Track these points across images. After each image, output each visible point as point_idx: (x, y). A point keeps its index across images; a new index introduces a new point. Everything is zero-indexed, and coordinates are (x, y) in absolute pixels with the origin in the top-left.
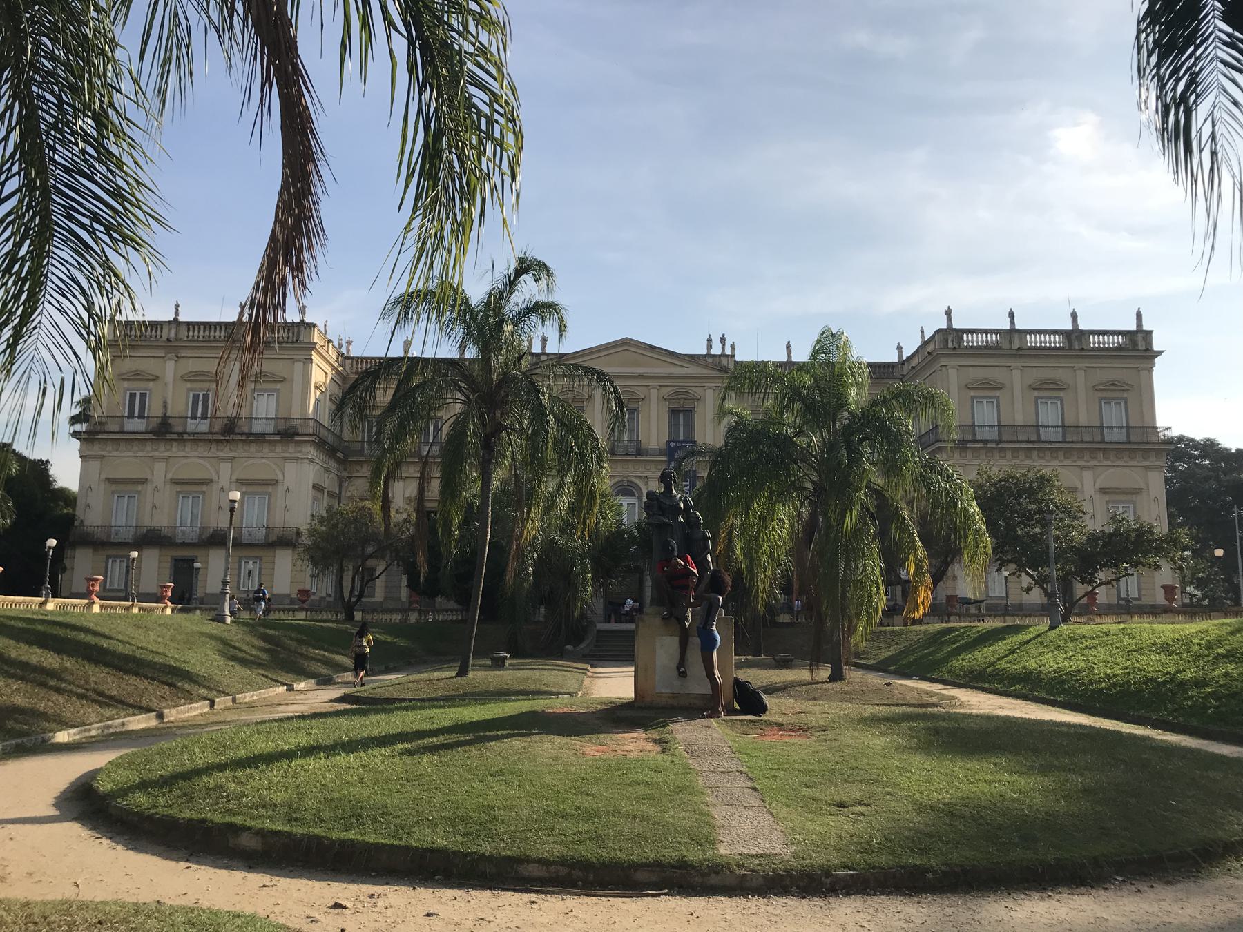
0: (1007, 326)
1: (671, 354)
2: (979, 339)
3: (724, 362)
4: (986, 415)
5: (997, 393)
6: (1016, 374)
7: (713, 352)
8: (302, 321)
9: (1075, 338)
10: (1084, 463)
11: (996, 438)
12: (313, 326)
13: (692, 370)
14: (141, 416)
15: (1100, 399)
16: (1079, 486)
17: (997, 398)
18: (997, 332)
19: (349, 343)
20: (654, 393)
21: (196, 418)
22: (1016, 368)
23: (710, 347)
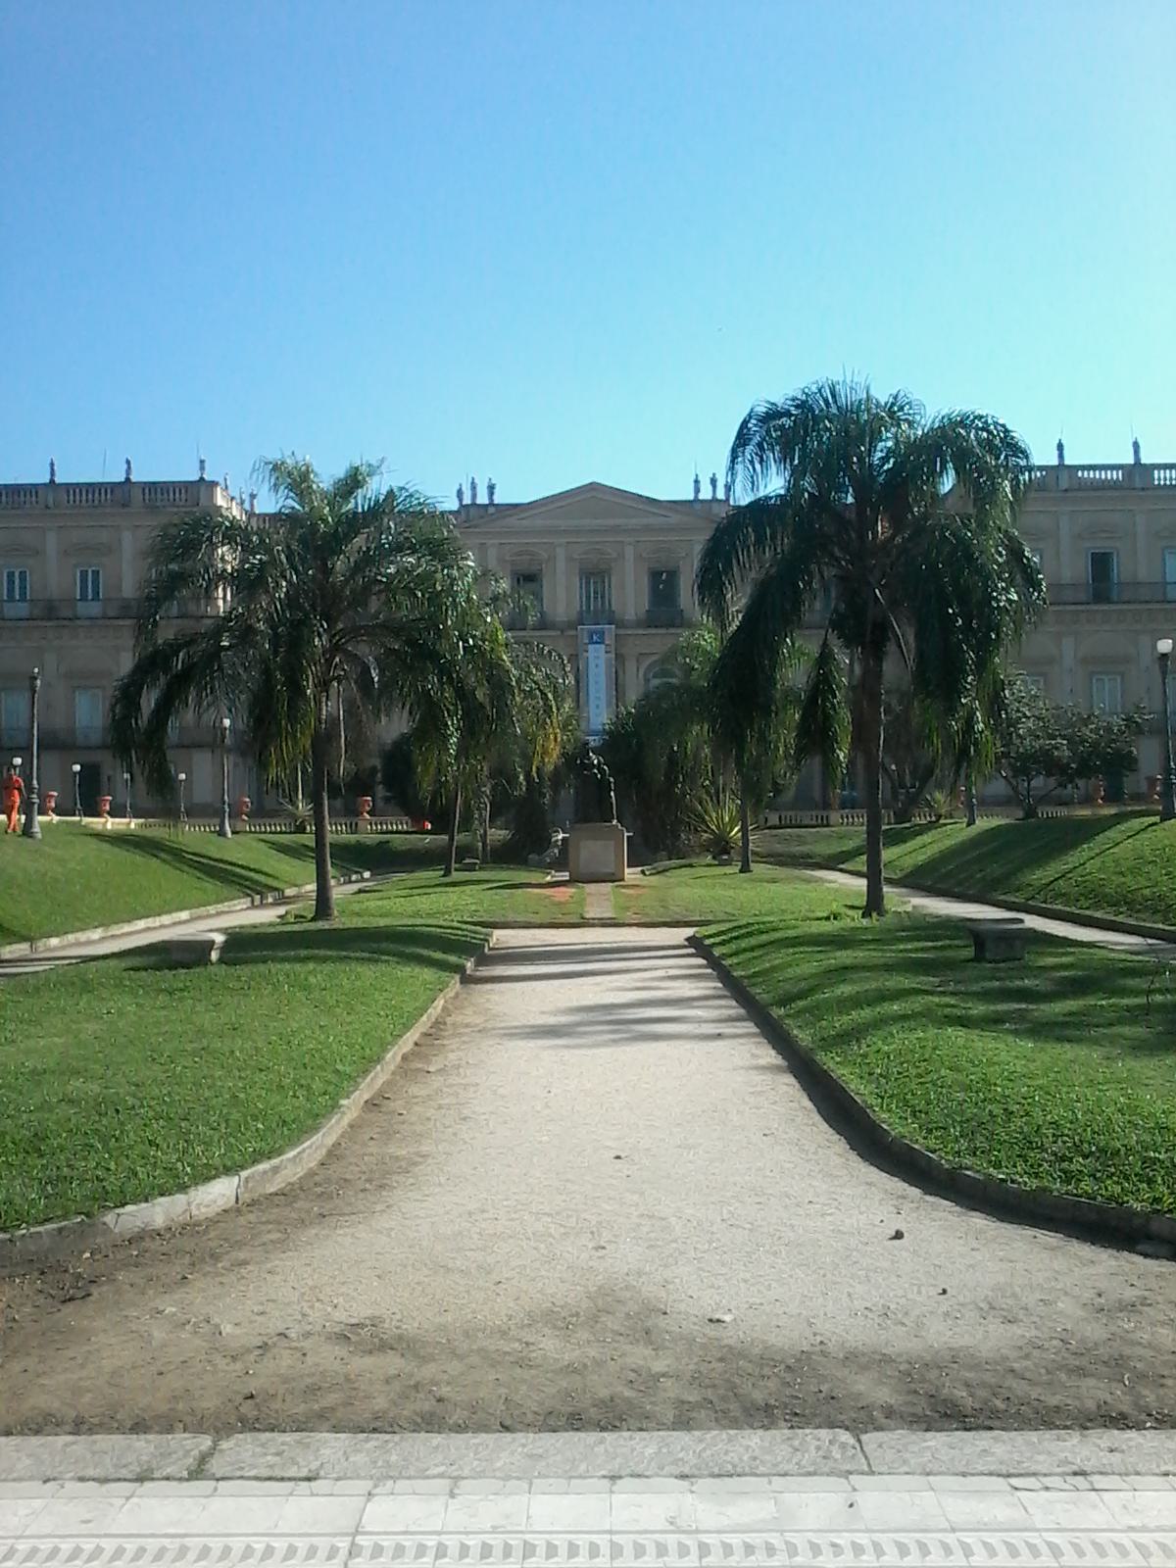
0: (1055, 462)
3: (716, 508)
7: (701, 496)
8: (202, 479)
9: (1138, 472)
12: (214, 484)
13: (674, 519)
14: (23, 599)
19: (253, 496)
20: (629, 552)
21: (87, 600)
23: (697, 490)
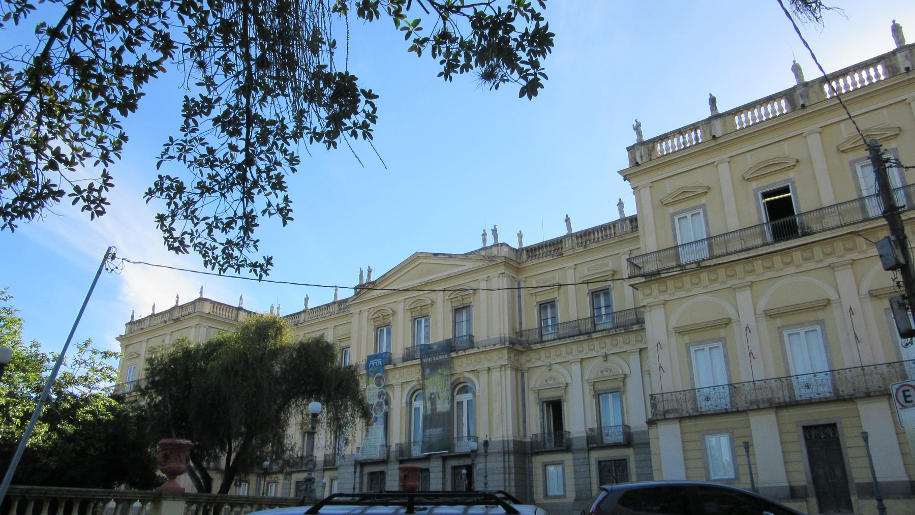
1: (450, 255)
2: (675, 144)
4: (691, 229)
5: (703, 200)
6: (724, 168)
10: (832, 260)
11: (706, 254)
13: (469, 265)
15: (852, 163)
16: (833, 296)
17: (703, 206)
18: (694, 127)
22: (722, 162)
23: (484, 241)
